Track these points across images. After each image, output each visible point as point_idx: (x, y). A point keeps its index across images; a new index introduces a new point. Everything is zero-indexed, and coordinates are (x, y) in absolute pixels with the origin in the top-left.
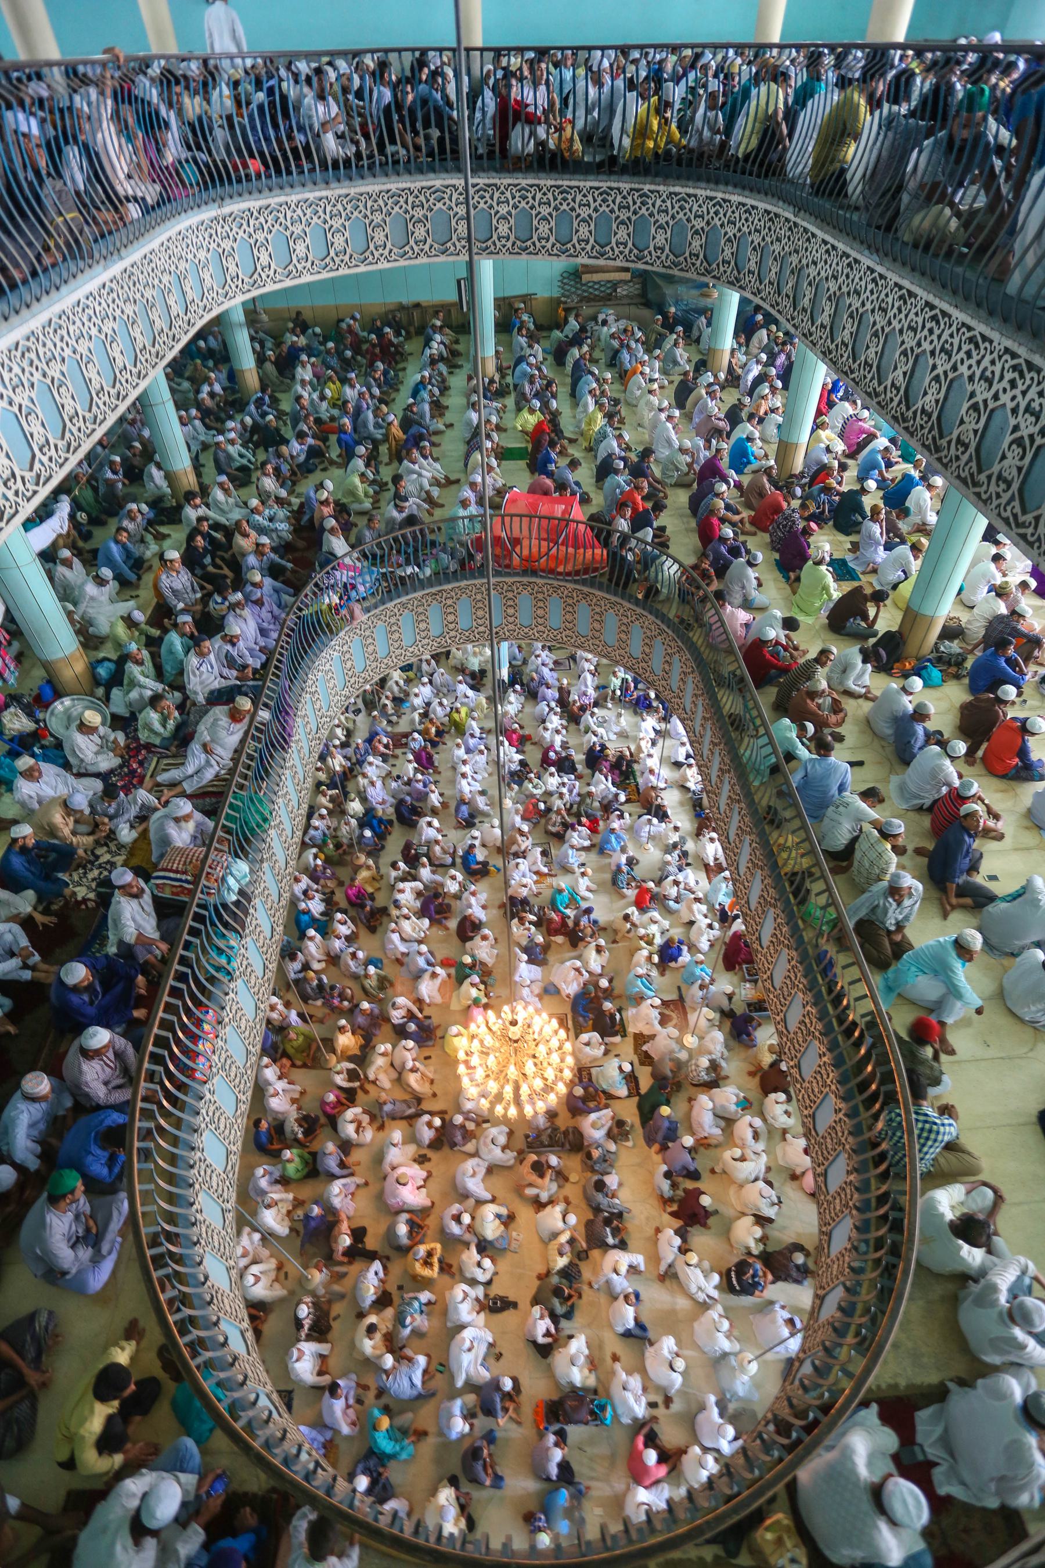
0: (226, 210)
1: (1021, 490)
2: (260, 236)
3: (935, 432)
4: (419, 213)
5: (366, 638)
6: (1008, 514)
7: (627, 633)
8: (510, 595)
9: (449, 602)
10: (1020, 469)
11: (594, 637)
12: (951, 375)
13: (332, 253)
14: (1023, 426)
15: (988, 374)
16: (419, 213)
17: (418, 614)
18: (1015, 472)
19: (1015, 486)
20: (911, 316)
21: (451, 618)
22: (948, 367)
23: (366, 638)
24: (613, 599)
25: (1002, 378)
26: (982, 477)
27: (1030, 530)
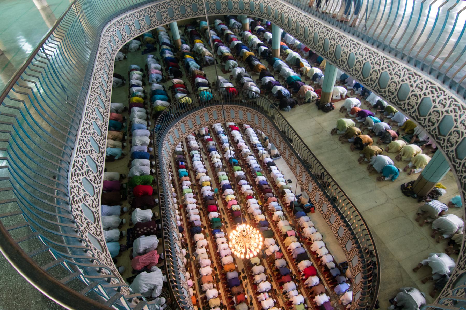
0: (112, 23)
1: (362, 73)
2: (122, 28)
3: (334, 58)
4: (164, 10)
5: (172, 134)
6: (360, 78)
7: (246, 115)
8: (210, 112)
9: (193, 118)
10: (361, 68)
11: (236, 118)
12: (336, 45)
13: (142, 27)
14: (359, 58)
15: (347, 45)
16: (164, 10)
17: (185, 123)
18: (359, 69)
19: (360, 72)
20: (321, 29)
21: (194, 122)
22: (335, 42)
23: (172, 134)
24: (240, 106)
25: (351, 46)
26: (351, 70)
27: (367, 82)
